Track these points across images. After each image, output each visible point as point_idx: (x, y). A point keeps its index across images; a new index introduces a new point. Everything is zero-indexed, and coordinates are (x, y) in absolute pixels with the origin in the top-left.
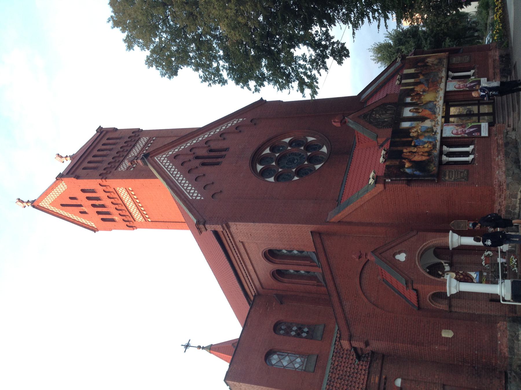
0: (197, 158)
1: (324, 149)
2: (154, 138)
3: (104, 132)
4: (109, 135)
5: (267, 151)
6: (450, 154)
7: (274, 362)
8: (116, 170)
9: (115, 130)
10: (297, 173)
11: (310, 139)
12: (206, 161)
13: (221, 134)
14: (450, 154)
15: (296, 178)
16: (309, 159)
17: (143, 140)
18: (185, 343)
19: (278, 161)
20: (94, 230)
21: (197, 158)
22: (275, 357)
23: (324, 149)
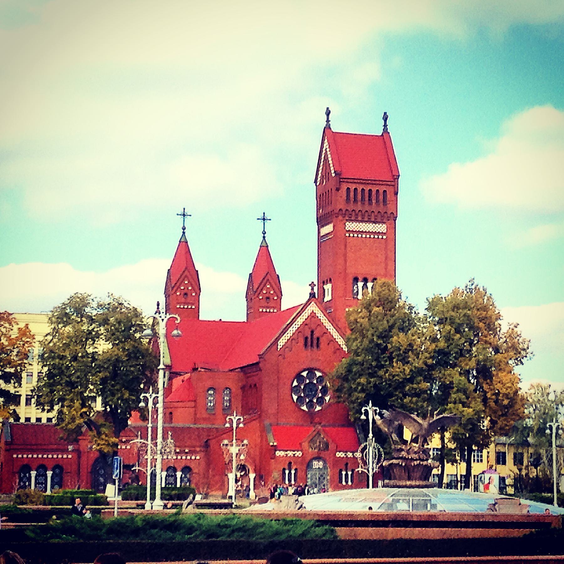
0: (312, 332)
1: (318, 408)
2: (384, 237)
3: (393, 183)
4: (390, 190)
5: (318, 374)
6: (290, 473)
7: (210, 392)
8: (347, 220)
9: (396, 194)
10: (299, 398)
11: (327, 398)
12: (309, 339)
13: (333, 340)
14: (290, 473)
15: (295, 397)
16: (311, 401)
17: (382, 228)
18: (267, 216)
19: (311, 383)
20: (316, 182)
21: (312, 332)
22: (212, 392)
23: (318, 408)
